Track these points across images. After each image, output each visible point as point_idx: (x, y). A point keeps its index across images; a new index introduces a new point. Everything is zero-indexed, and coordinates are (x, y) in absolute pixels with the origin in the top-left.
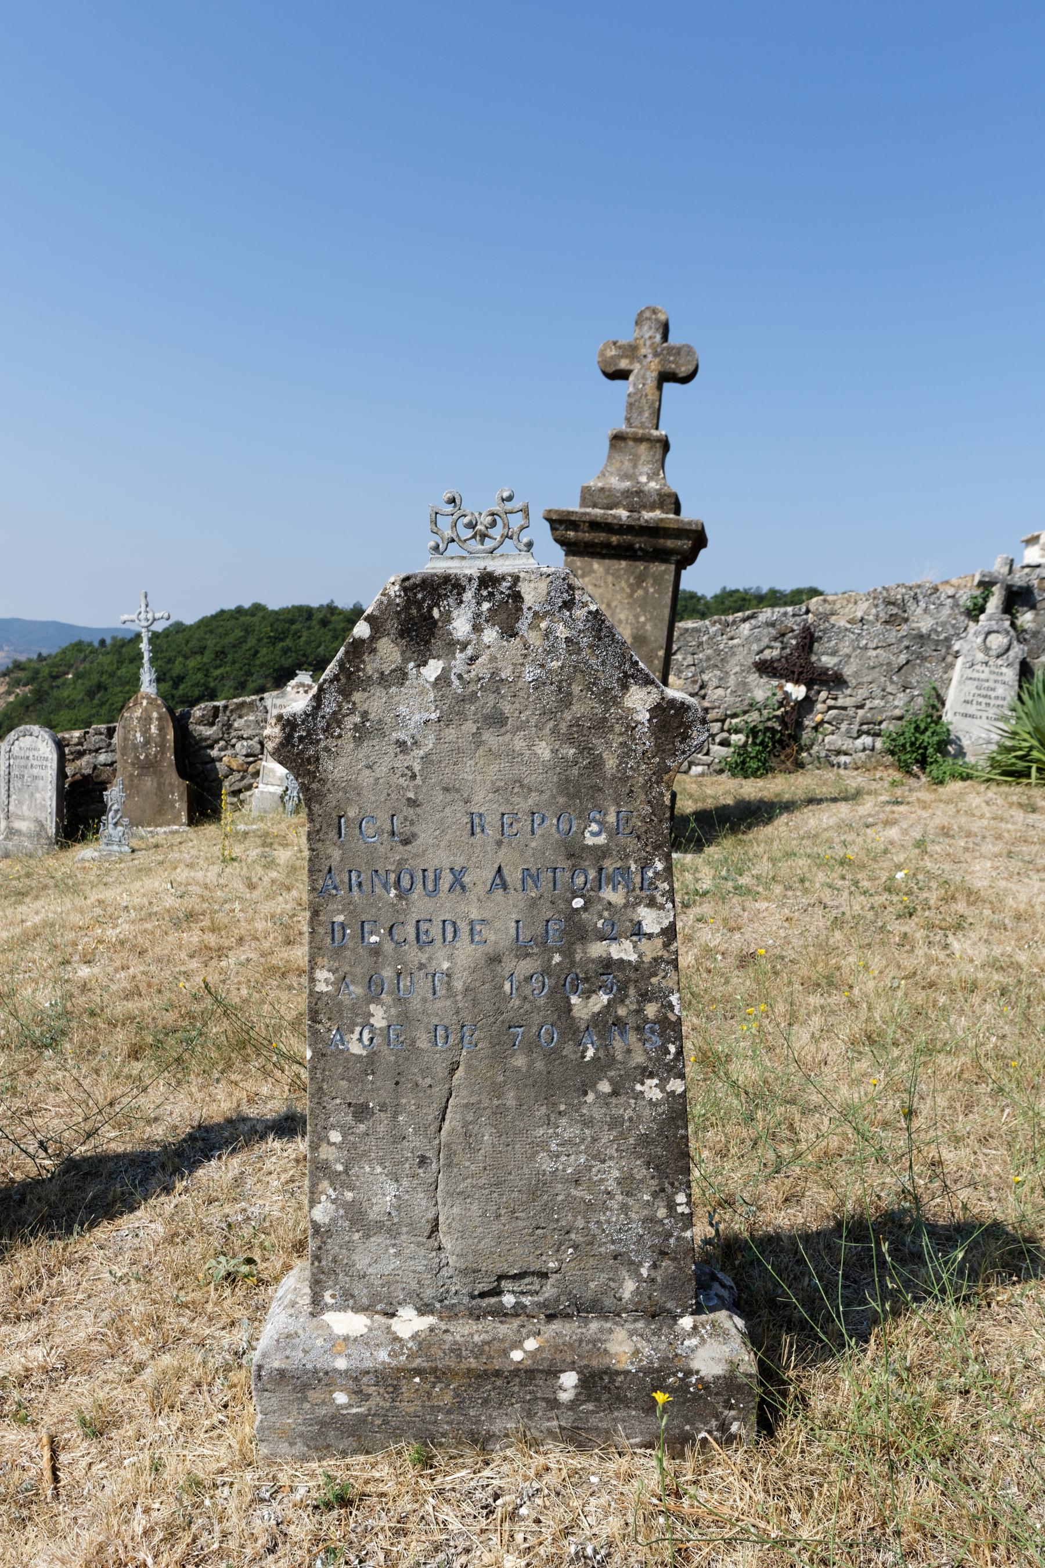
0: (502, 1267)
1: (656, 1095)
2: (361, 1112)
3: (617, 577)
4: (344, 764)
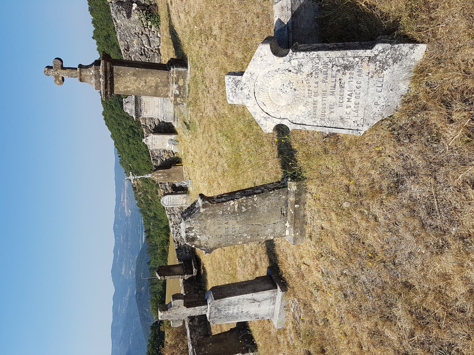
0: (280, 214)
1: (256, 198)
2: (258, 235)
3: (118, 81)
4: (211, 245)
